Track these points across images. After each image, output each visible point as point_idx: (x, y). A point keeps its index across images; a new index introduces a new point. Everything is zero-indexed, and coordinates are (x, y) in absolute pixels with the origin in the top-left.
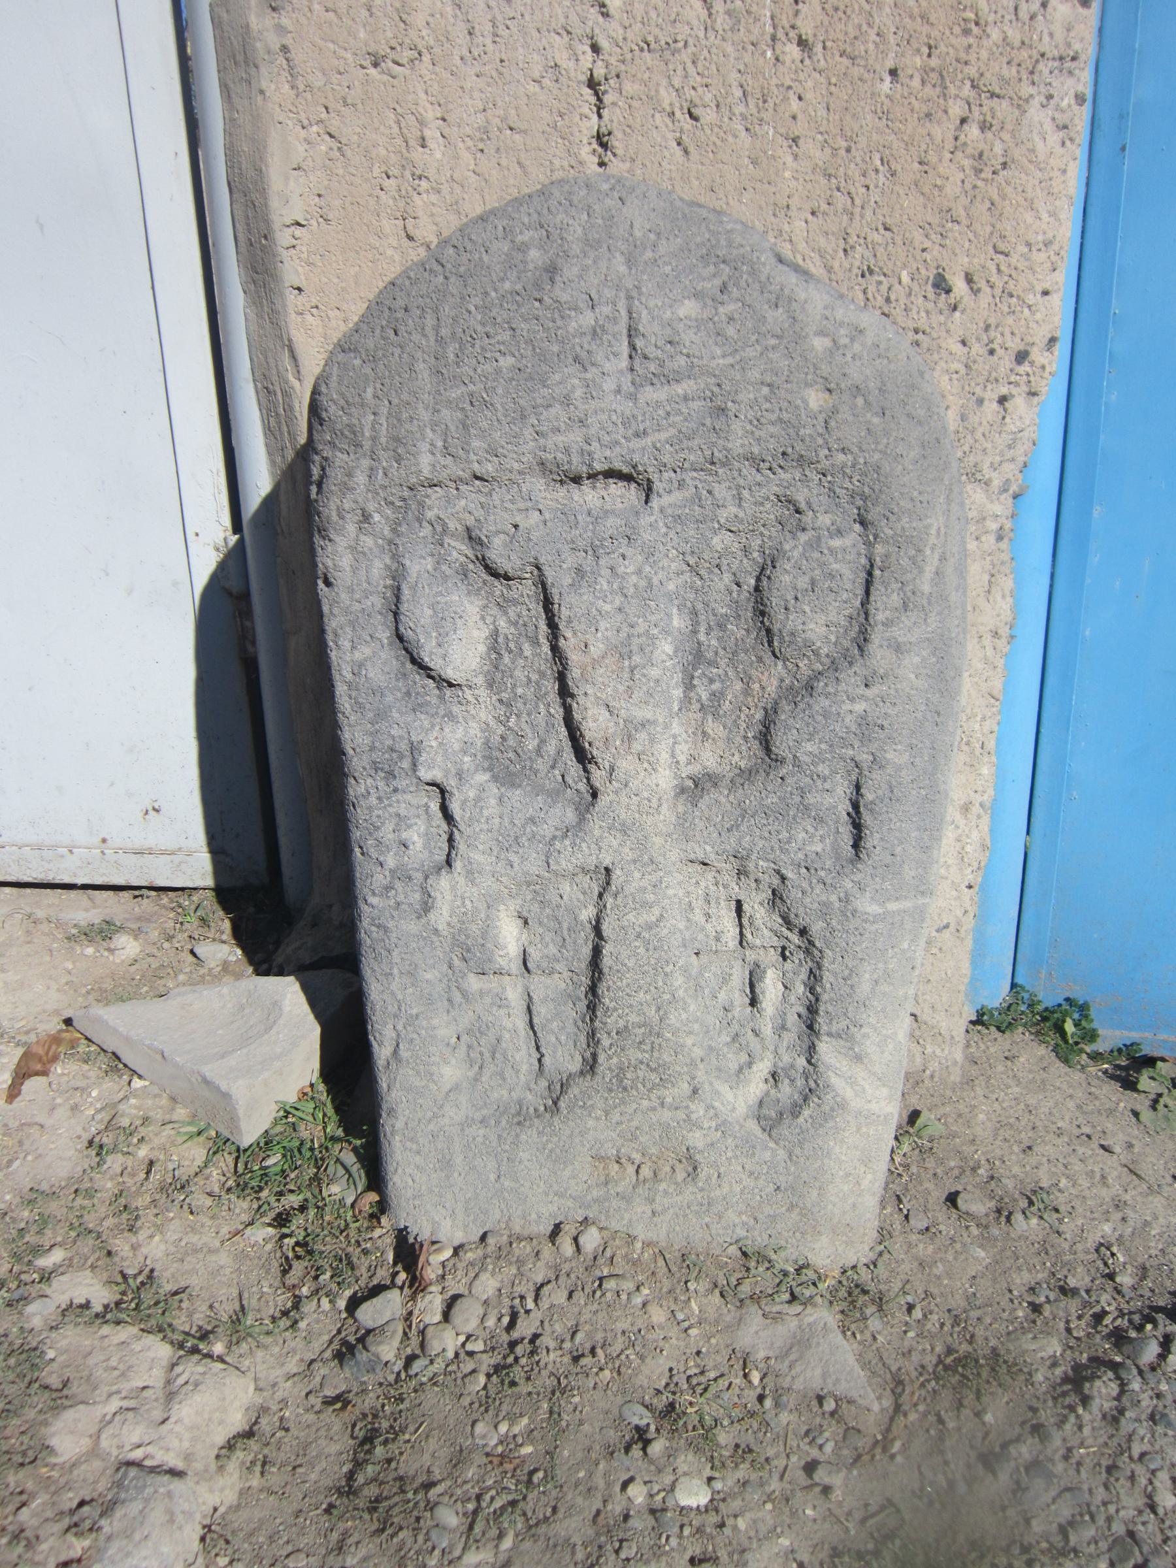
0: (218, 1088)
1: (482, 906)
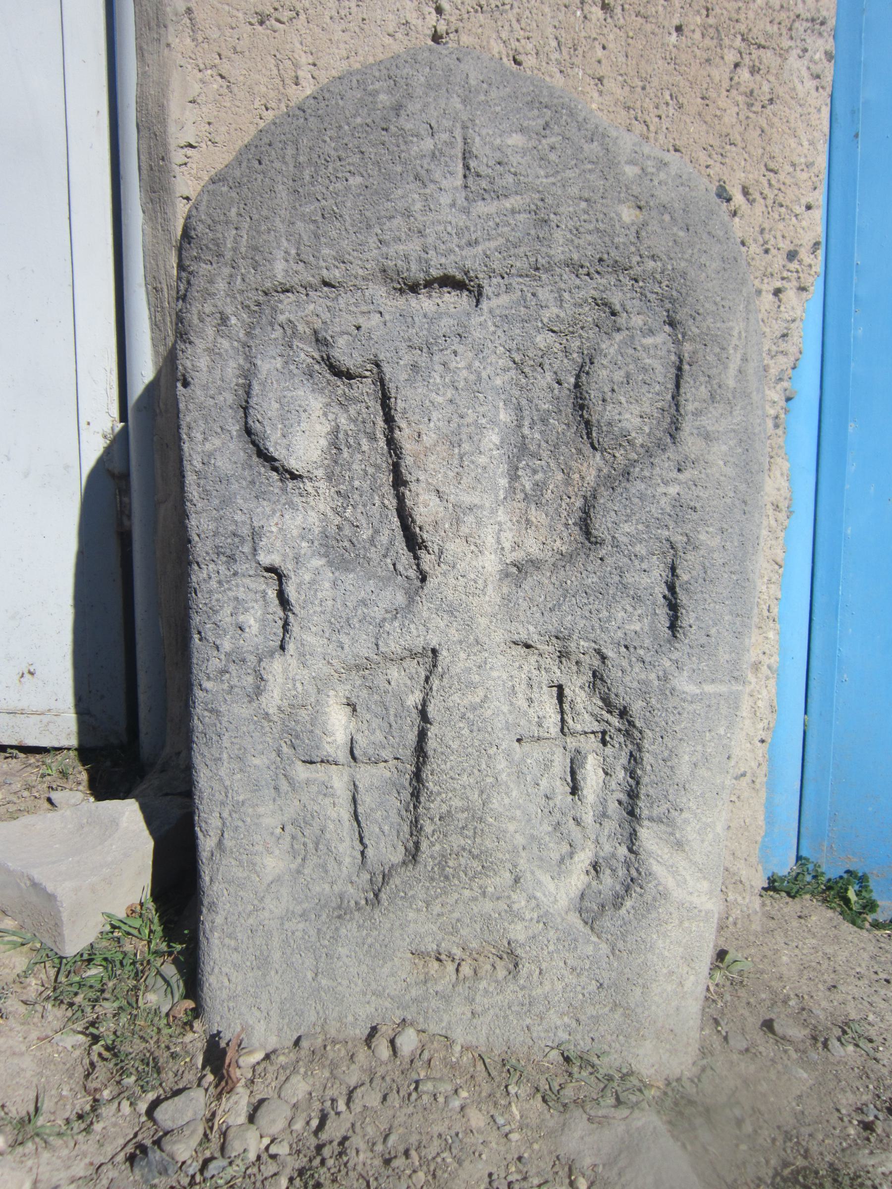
0: (44, 890)
1: (312, 690)
